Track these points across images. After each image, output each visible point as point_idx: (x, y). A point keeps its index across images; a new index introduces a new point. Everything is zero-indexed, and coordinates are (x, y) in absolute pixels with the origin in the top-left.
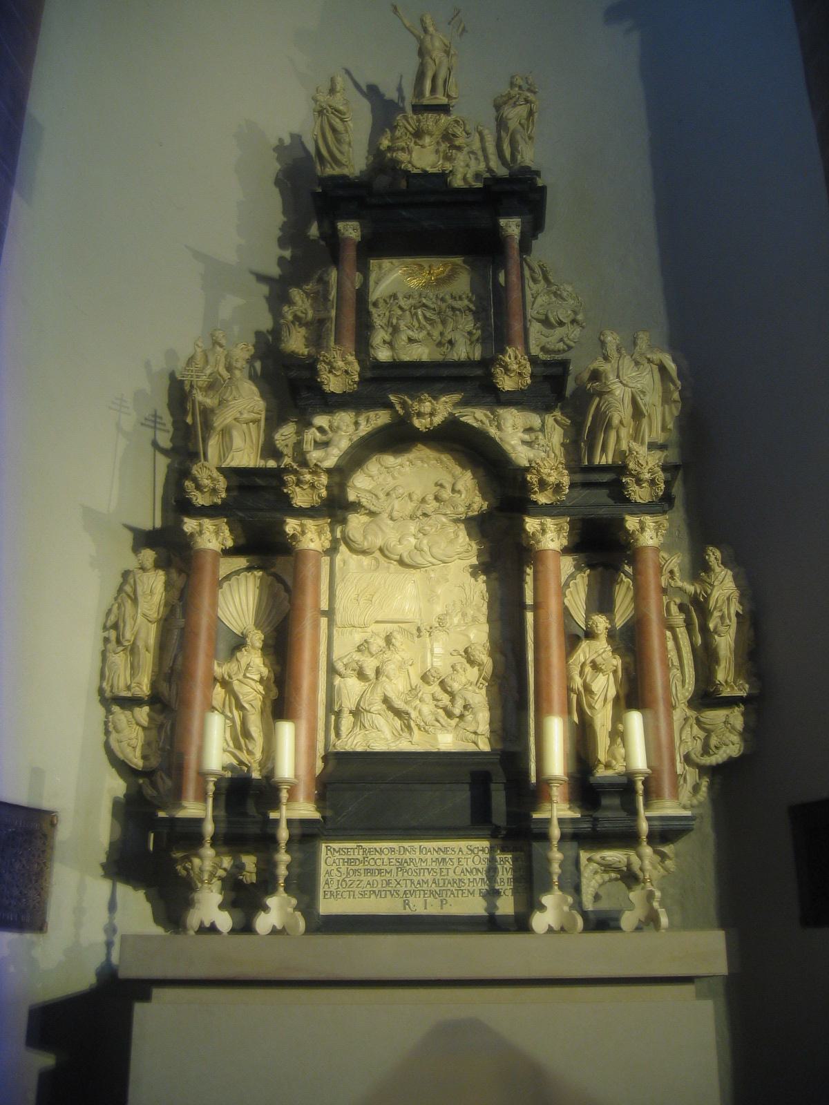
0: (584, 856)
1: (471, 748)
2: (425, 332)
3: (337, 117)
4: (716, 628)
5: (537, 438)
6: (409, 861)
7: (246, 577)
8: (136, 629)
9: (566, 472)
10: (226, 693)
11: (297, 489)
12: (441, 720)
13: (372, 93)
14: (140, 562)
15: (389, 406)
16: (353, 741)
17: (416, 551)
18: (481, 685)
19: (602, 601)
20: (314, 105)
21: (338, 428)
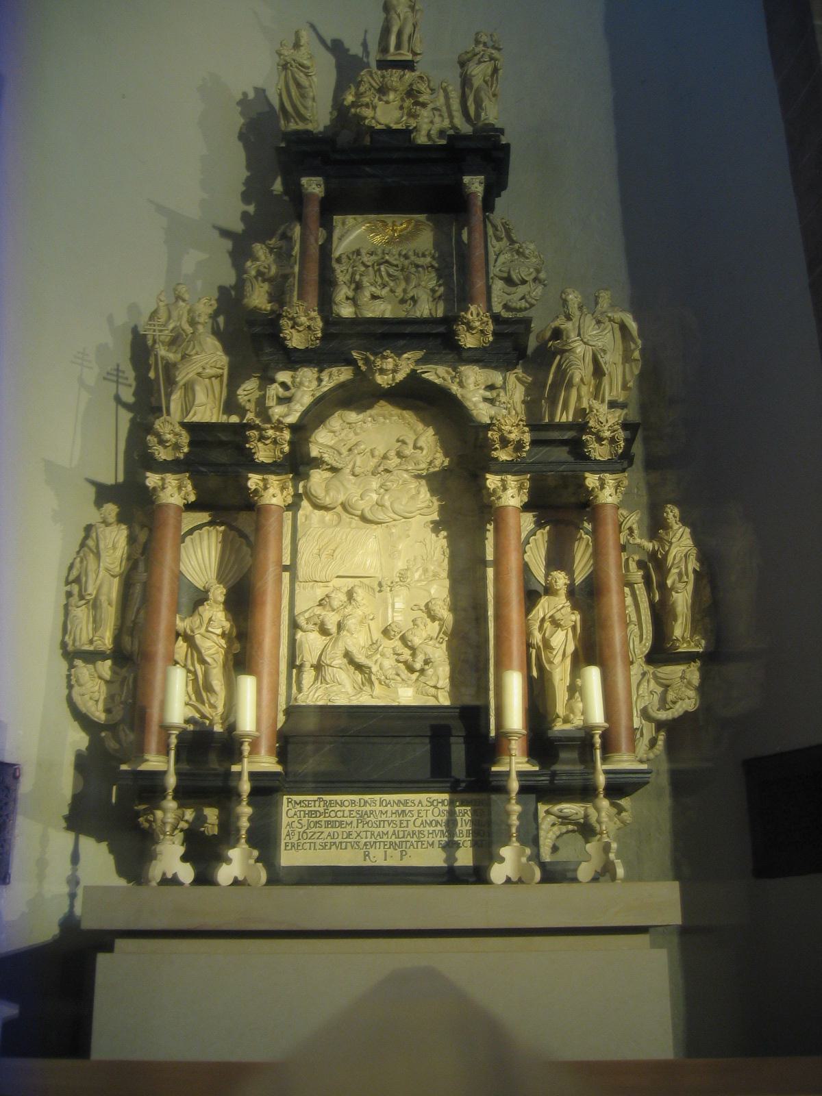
0: (542, 808)
1: (431, 702)
2: (387, 289)
3: (302, 71)
4: (673, 583)
5: (498, 395)
6: (369, 812)
7: (209, 532)
8: (98, 582)
9: (526, 429)
10: (188, 647)
11: (260, 445)
12: (402, 674)
13: (336, 48)
14: (102, 516)
15: (350, 362)
16: (313, 694)
17: (377, 506)
18: (441, 640)
19: (559, 558)
20: (277, 59)
21: (301, 384)
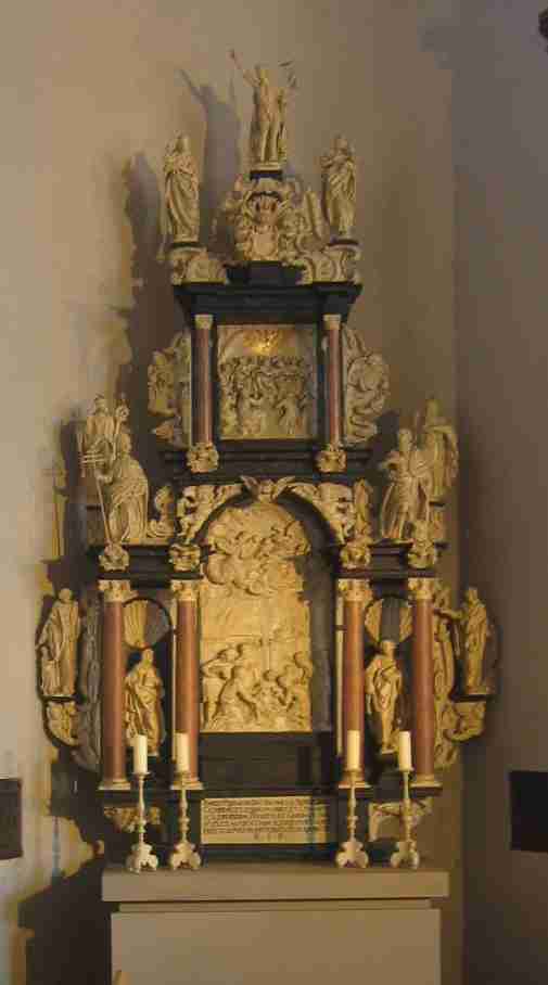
1: (298, 728)
7: (136, 605)
9: (368, 549)
11: (179, 560)
15: (239, 481)
16: (215, 726)
19: (388, 624)
21: (203, 499)
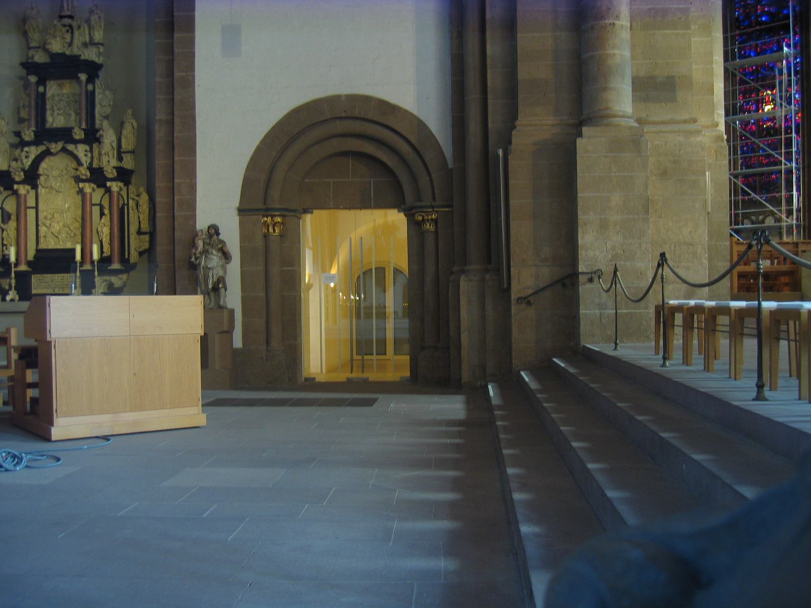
15: (44, 144)
